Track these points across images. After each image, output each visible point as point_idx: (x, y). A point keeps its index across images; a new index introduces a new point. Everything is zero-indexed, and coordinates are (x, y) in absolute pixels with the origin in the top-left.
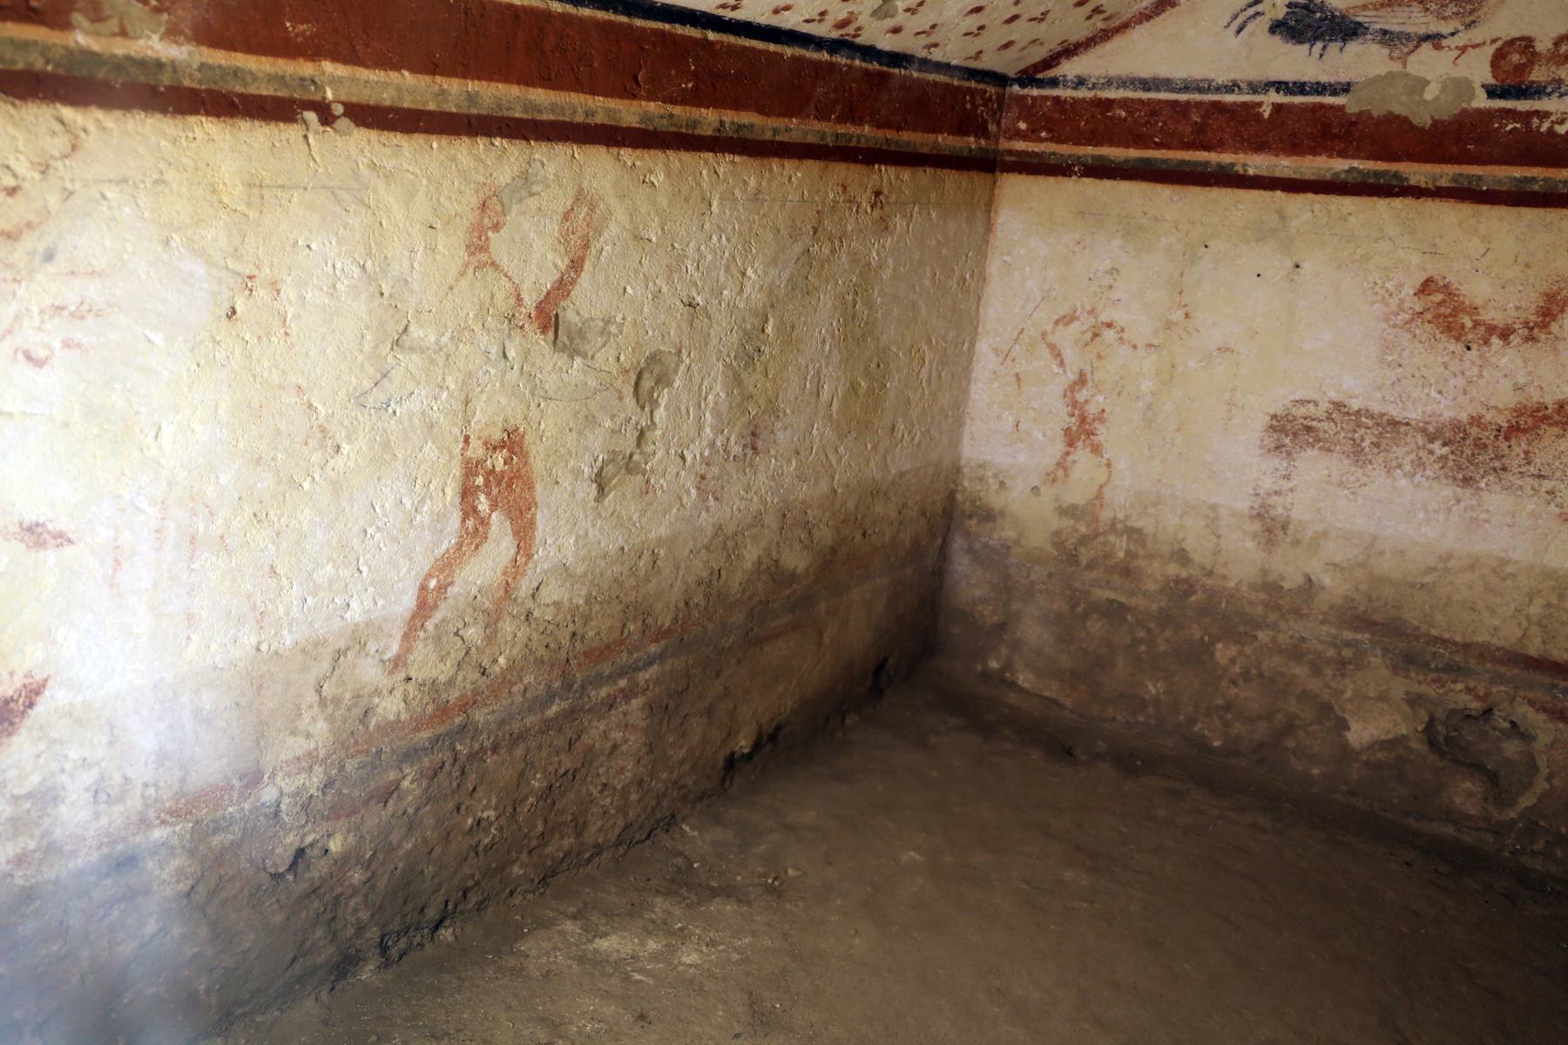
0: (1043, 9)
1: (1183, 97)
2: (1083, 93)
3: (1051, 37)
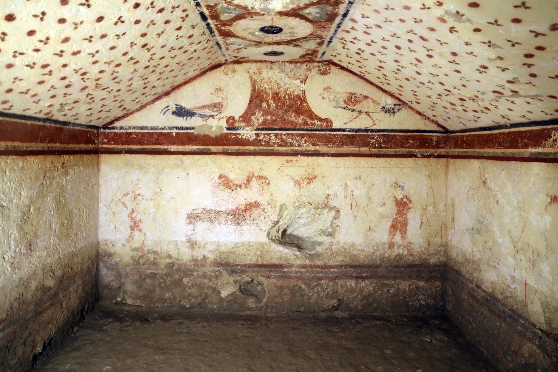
0: (109, 108)
1: (151, 131)
2: (122, 131)
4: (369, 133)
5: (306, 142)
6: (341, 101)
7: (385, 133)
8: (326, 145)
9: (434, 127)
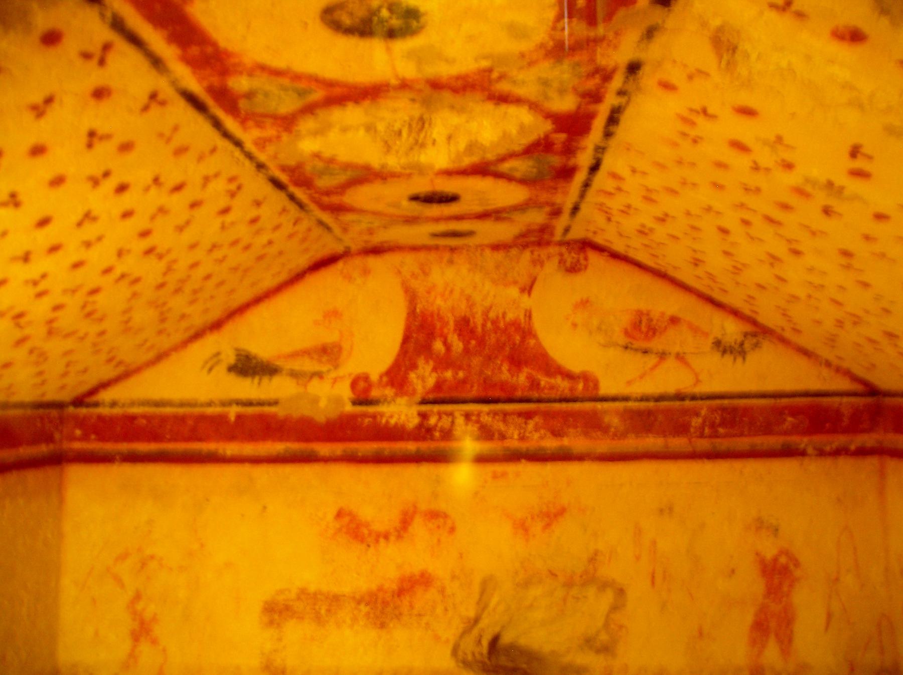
2: (117, 411)
3: (91, 380)
4: (687, 403)
5: (536, 429)
6: (617, 329)
7: (726, 402)
8: (586, 434)
9: (844, 384)
